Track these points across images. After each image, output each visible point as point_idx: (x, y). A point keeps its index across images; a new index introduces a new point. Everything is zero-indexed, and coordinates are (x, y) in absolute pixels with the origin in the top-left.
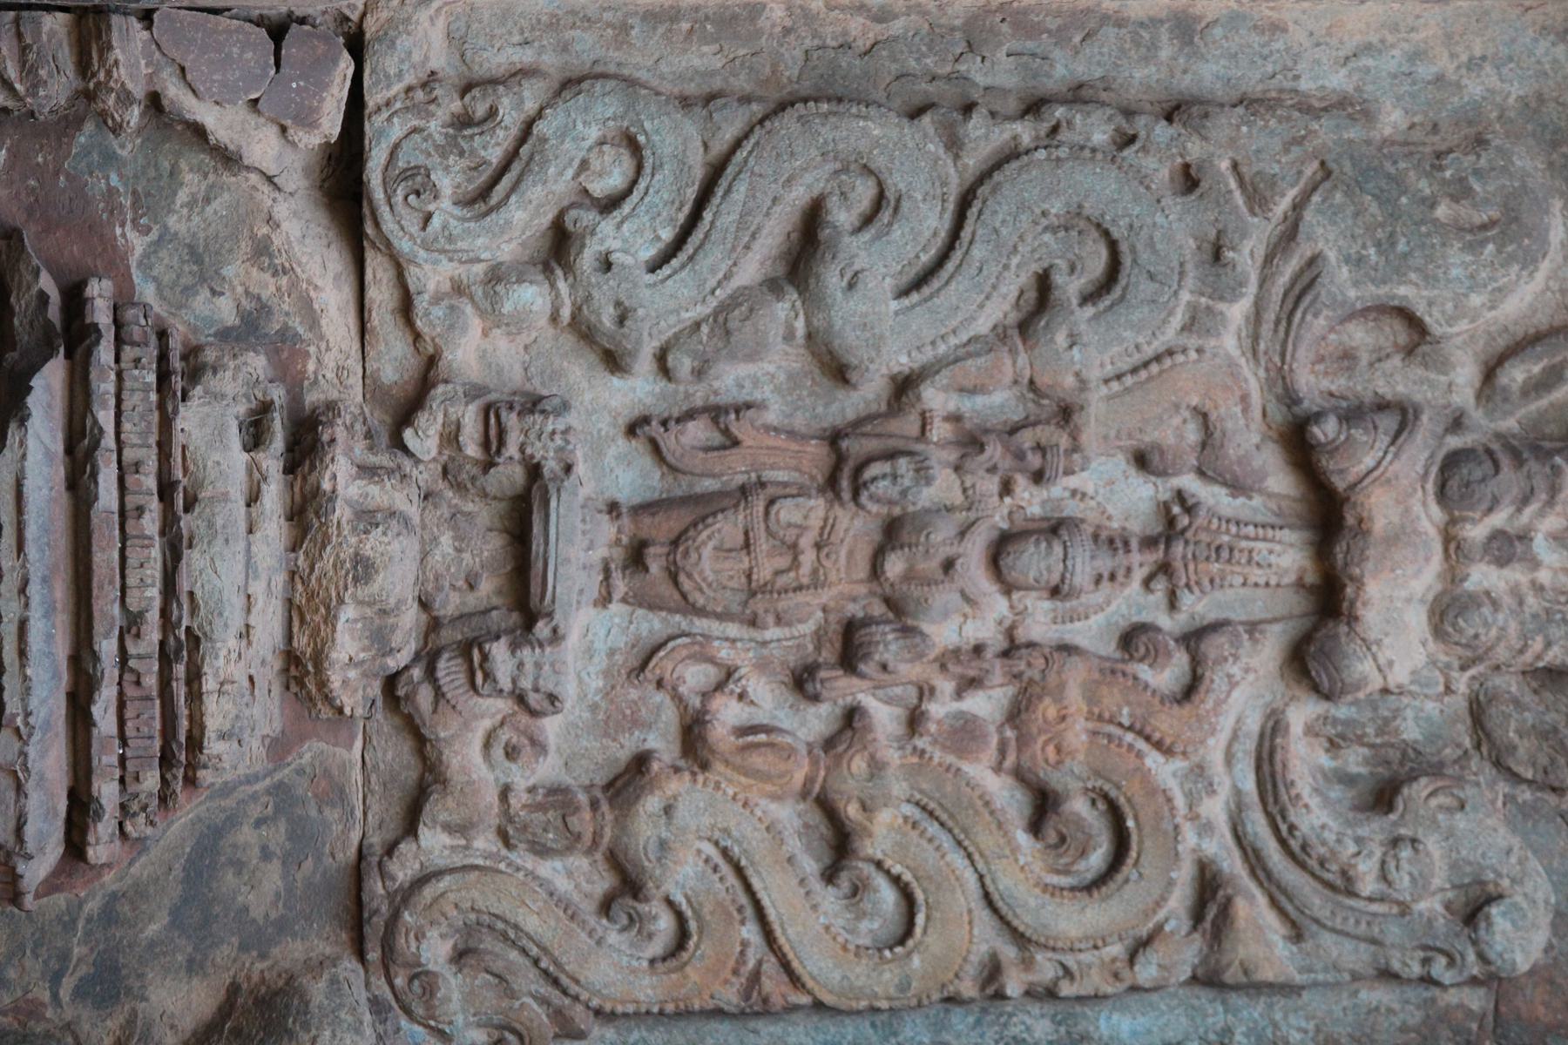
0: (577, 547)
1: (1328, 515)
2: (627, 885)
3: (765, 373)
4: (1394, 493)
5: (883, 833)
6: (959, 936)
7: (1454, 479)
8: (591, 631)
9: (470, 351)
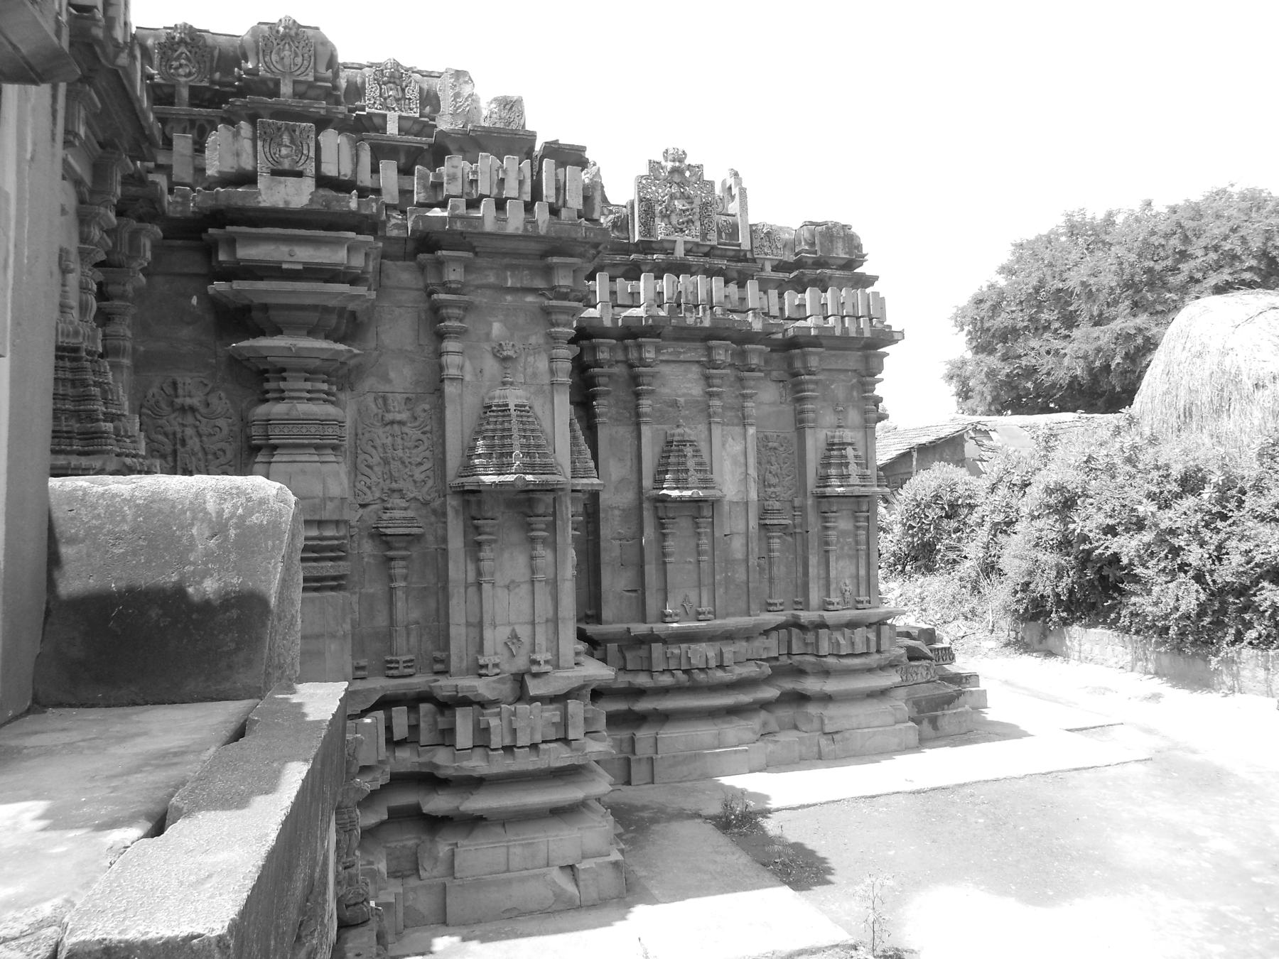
0: (394, 485)
4: (389, 417)
5: (419, 460)
6: (428, 454)
7: (388, 411)
9: (377, 495)
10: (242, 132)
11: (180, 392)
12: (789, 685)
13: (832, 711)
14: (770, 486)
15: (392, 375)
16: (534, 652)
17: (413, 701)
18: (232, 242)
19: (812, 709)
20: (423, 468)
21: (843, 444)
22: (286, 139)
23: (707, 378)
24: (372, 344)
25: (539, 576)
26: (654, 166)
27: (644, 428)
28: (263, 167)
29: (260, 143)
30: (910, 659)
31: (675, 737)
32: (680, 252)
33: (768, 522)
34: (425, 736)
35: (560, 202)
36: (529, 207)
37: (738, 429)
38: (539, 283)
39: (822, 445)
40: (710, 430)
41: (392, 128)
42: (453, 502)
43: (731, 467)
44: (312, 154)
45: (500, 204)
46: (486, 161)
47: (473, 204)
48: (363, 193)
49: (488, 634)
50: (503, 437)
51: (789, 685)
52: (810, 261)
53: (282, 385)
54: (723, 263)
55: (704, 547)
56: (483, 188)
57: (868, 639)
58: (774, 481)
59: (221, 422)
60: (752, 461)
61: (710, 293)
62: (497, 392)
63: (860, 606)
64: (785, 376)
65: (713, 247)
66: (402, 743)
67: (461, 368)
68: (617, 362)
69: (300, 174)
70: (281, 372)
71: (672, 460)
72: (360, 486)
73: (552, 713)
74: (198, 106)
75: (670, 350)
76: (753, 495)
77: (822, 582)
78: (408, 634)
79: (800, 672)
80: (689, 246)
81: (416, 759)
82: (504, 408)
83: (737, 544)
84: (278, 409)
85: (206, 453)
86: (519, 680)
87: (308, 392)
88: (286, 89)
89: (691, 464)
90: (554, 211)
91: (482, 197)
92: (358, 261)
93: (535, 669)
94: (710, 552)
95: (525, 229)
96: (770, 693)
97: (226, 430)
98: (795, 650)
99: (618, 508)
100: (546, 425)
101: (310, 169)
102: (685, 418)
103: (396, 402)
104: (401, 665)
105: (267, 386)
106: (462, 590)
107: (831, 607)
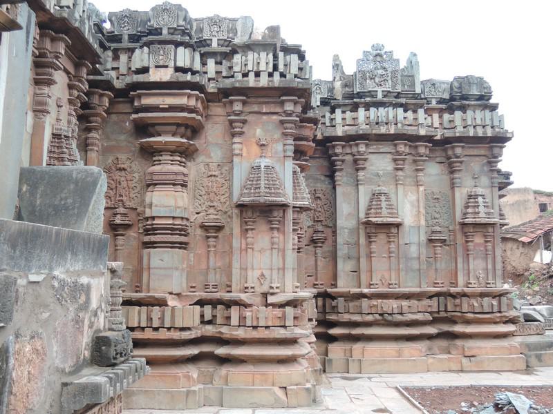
0: (212, 204)
1: (211, 176)
2: (225, 202)
3: (205, 197)
4: (210, 173)
6: (227, 190)
8: (215, 204)
10: (145, 51)
11: (119, 162)
12: (446, 328)
13: (470, 344)
14: (435, 218)
15: (212, 155)
16: (271, 283)
17: (214, 303)
18: (139, 96)
19: (459, 343)
20: (225, 196)
21: (477, 195)
22: (162, 52)
23: (395, 160)
24: (204, 141)
25: (276, 246)
26: (366, 53)
27: (361, 187)
28: (152, 65)
29: (151, 55)
30: (526, 321)
31: (373, 348)
32: (380, 96)
33: (433, 238)
34: (219, 321)
35: (288, 71)
36: (270, 75)
37: (414, 188)
38: (278, 110)
39: (465, 196)
40: (397, 188)
41: (215, 44)
42: (236, 211)
43: (409, 208)
44: (173, 58)
45: (257, 74)
46: (251, 56)
47: (245, 75)
48: (194, 73)
49: (250, 273)
50: (258, 180)
51: (446, 328)
52: (458, 97)
53: (160, 158)
54: (403, 101)
55: (393, 250)
56: (250, 68)
57: (492, 305)
58: (437, 216)
59: (136, 175)
60: (422, 204)
61: (395, 117)
62: (257, 161)
63: (488, 286)
64: (443, 160)
65: (399, 93)
66: (209, 322)
67: (241, 150)
68: (347, 154)
69: (166, 67)
70: (159, 152)
71: (374, 203)
72: (197, 204)
73: (278, 312)
74: (132, 42)
75: (375, 147)
76: (423, 222)
77: (466, 272)
78: (215, 273)
79: (453, 321)
80: (385, 93)
81: (215, 330)
82: (259, 167)
83: (413, 250)
84: (157, 168)
85: (129, 188)
86: (265, 295)
87: (172, 161)
88: (165, 31)
89: (384, 205)
90: (283, 75)
91: (249, 71)
92: (192, 102)
93: (271, 291)
94: (396, 251)
95: (268, 84)
96: (431, 330)
97: (137, 178)
98: (449, 309)
99: (346, 228)
100: (281, 176)
101: (172, 64)
102: (383, 182)
103: (213, 166)
104: (211, 287)
105: (154, 159)
106: (239, 252)
107: (470, 286)
